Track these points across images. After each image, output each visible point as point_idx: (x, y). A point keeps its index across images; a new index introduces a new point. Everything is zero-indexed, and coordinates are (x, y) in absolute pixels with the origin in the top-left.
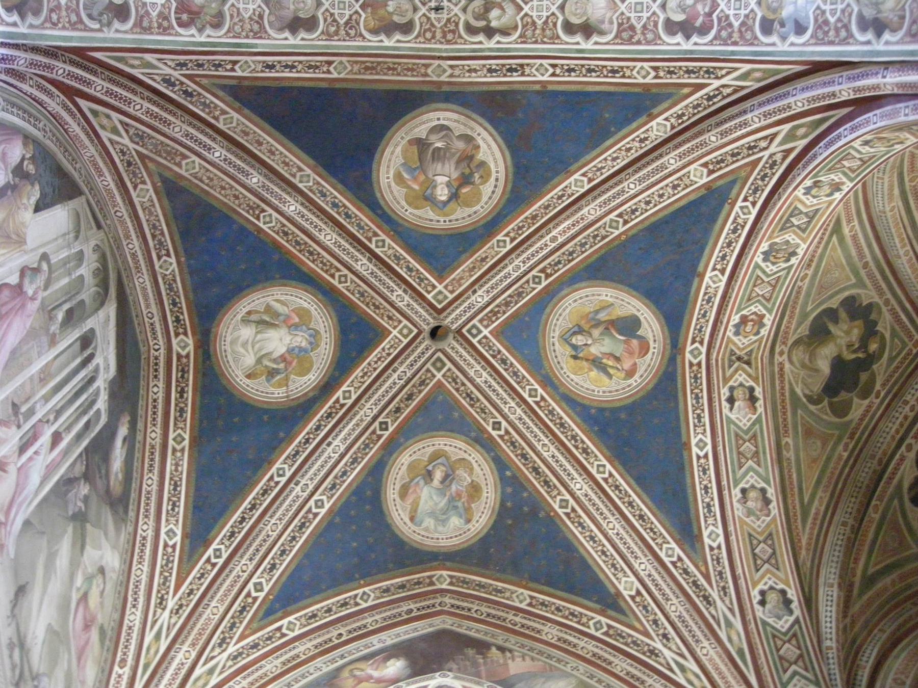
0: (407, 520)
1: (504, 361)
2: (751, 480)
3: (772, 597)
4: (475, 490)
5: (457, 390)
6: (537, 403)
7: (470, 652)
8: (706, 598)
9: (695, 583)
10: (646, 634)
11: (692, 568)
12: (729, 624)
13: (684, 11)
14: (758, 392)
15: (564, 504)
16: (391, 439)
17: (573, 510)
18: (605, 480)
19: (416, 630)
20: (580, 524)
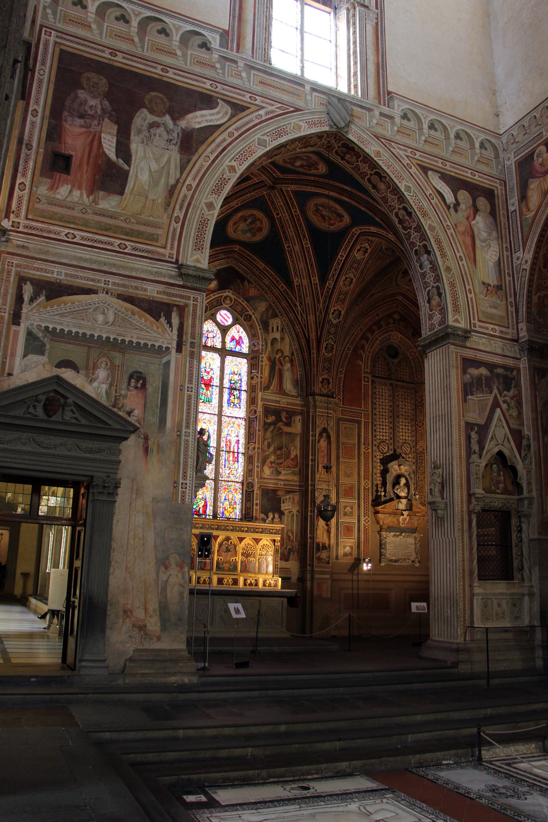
0: (232, 232)
1: (291, 199)
2: (351, 275)
3: (337, 312)
4: (260, 229)
5: (269, 199)
6: (296, 215)
7: (239, 281)
8: (318, 300)
9: (318, 294)
10: (296, 299)
11: (319, 289)
12: (321, 312)
13: (403, 217)
14: (369, 251)
15: (289, 247)
16: (238, 208)
17: (291, 250)
18: (306, 248)
19: (222, 264)
20: (291, 256)
